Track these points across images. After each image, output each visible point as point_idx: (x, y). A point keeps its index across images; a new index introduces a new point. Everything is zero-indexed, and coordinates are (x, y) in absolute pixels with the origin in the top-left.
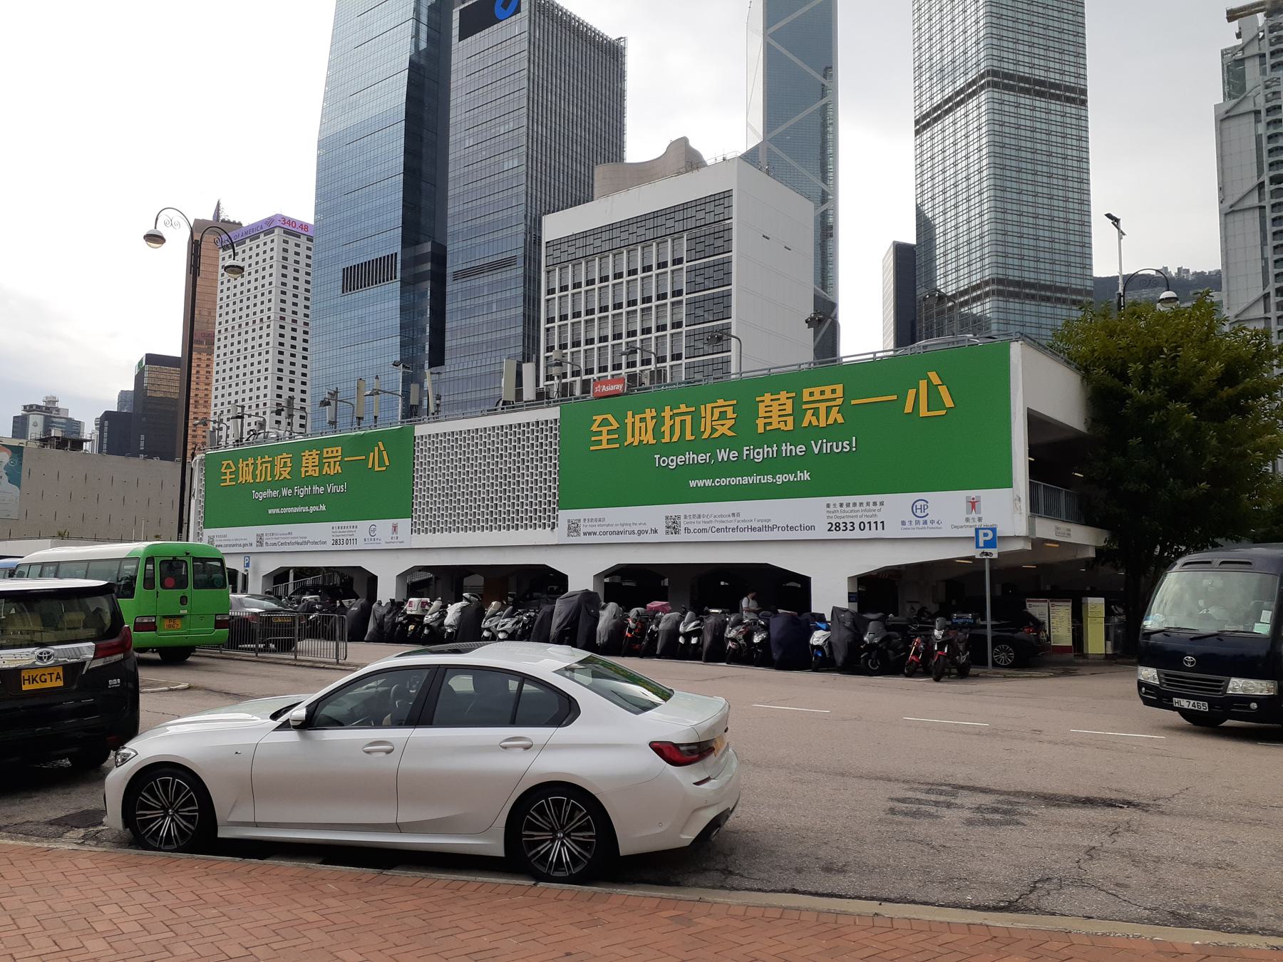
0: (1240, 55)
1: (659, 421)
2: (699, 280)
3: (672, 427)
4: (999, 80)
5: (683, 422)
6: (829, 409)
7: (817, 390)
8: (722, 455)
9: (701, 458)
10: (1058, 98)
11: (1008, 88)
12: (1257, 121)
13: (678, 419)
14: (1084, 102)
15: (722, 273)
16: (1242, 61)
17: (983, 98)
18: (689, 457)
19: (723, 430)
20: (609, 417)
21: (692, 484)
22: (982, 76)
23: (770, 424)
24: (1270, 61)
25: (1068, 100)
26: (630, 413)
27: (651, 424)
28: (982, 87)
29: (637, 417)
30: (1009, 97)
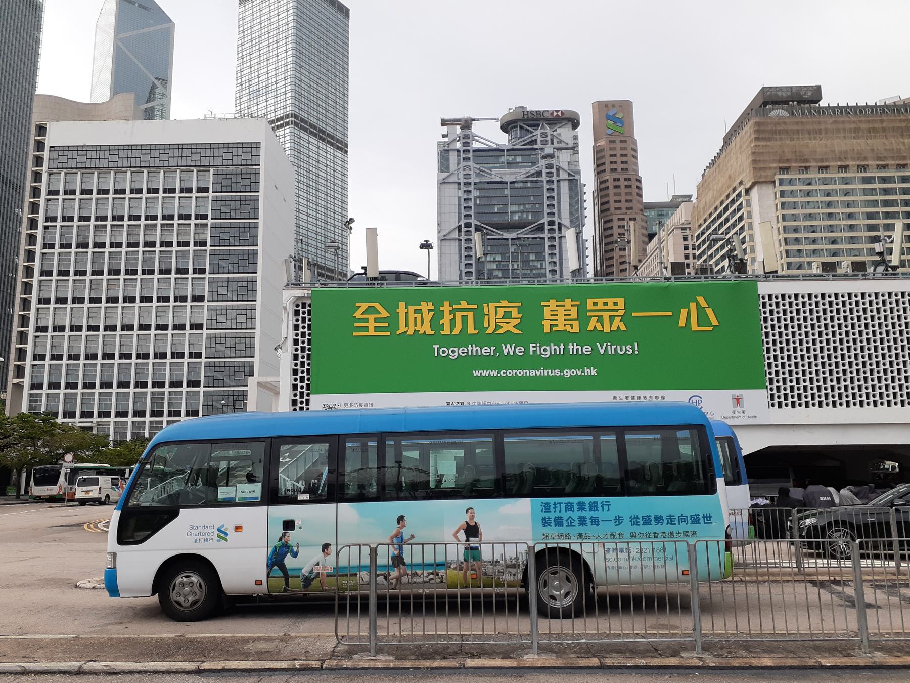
0: (446, 147)
1: (437, 315)
2: (224, 209)
3: (452, 321)
4: (298, 122)
5: (464, 318)
6: (612, 318)
7: (600, 302)
8: (508, 349)
9: (485, 351)
10: (332, 144)
11: (303, 128)
12: (459, 189)
13: (458, 315)
14: (346, 152)
15: (251, 208)
16: (448, 151)
17: (288, 131)
18: (473, 349)
19: (509, 326)
20: (377, 306)
21: (476, 374)
22: (288, 116)
23: (557, 325)
24: (463, 155)
25: (338, 147)
26: (402, 305)
27: (428, 317)
28: (287, 124)
29: (412, 309)
30: (304, 135)
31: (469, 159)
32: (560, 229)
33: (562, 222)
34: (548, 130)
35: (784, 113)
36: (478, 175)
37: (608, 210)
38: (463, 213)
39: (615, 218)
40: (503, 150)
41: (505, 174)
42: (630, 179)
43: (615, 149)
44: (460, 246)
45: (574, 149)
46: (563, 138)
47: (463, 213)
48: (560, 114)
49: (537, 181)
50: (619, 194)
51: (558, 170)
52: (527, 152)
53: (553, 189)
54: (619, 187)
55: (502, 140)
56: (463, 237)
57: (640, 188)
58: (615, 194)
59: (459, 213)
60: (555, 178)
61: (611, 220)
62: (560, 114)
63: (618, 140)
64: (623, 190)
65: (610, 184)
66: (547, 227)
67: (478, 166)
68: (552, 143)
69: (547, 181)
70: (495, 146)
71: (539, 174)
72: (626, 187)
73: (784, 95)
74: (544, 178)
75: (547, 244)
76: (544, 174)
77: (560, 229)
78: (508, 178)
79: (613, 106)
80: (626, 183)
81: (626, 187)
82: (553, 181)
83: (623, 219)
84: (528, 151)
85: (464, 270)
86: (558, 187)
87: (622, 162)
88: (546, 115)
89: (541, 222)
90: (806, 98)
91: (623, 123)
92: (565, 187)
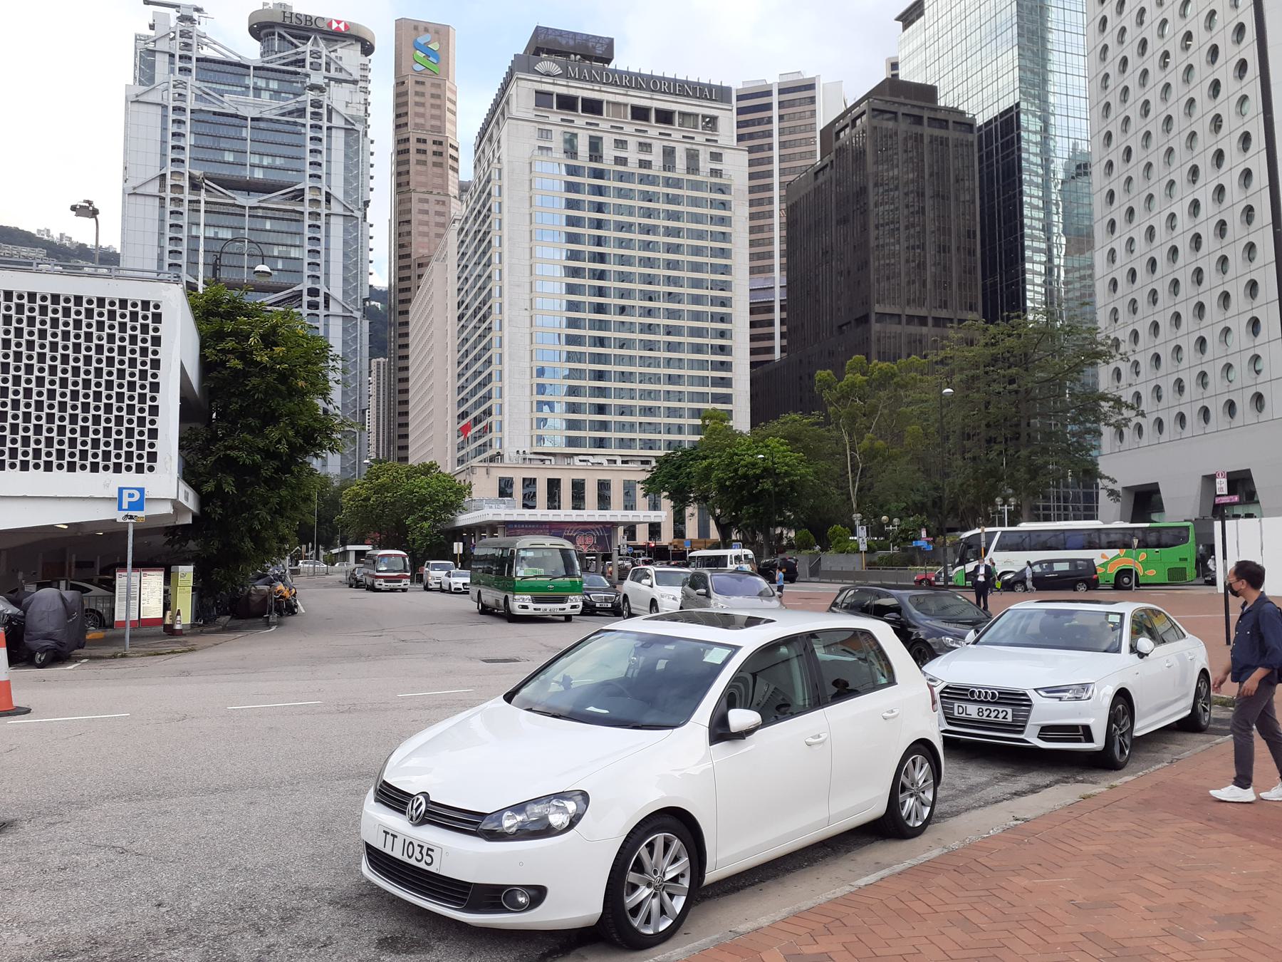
0: (151, 46)
31: (190, 71)
32: (328, 201)
34: (322, 47)
35: (557, 70)
36: (198, 98)
38: (171, 155)
39: (414, 196)
40: (248, 67)
41: (246, 104)
42: (441, 143)
43: (423, 95)
44: (162, 206)
45: (359, 82)
46: (343, 64)
47: (171, 155)
48: (342, 27)
49: (295, 124)
50: (424, 163)
51: (330, 112)
52: (288, 77)
53: (320, 140)
54: (425, 152)
55: (251, 51)
56: (169, 194)
57: (456, 160)
58: (418, 162)
59: (163, 155)
60: (325, 124)
62: (342, 27)
63: (428, 82)
64: (430, 158)
65: (413, 145)
66: (308, 196)
67: (198, 84)
68: (328, 70)
69: (312, 126)
70: (236, 59)
71: (301, 112)
72: (435, 153)
73: (564, 42)
74: (308, 121)
75: (307, 222)
76: (308, 115)
77: (328, 201)
78: (251, 113)
79: (426, 30)
80: (435, 148)
81: (435, 153)
82: (321, 128)
84: (288, 74)
85: (168, 247)
86: (329, 136)
87: (433, 117)
88: (320, 24)
89: (297, 187)
90: (591, 54)
91: (437, 57)
92: (339, 138)
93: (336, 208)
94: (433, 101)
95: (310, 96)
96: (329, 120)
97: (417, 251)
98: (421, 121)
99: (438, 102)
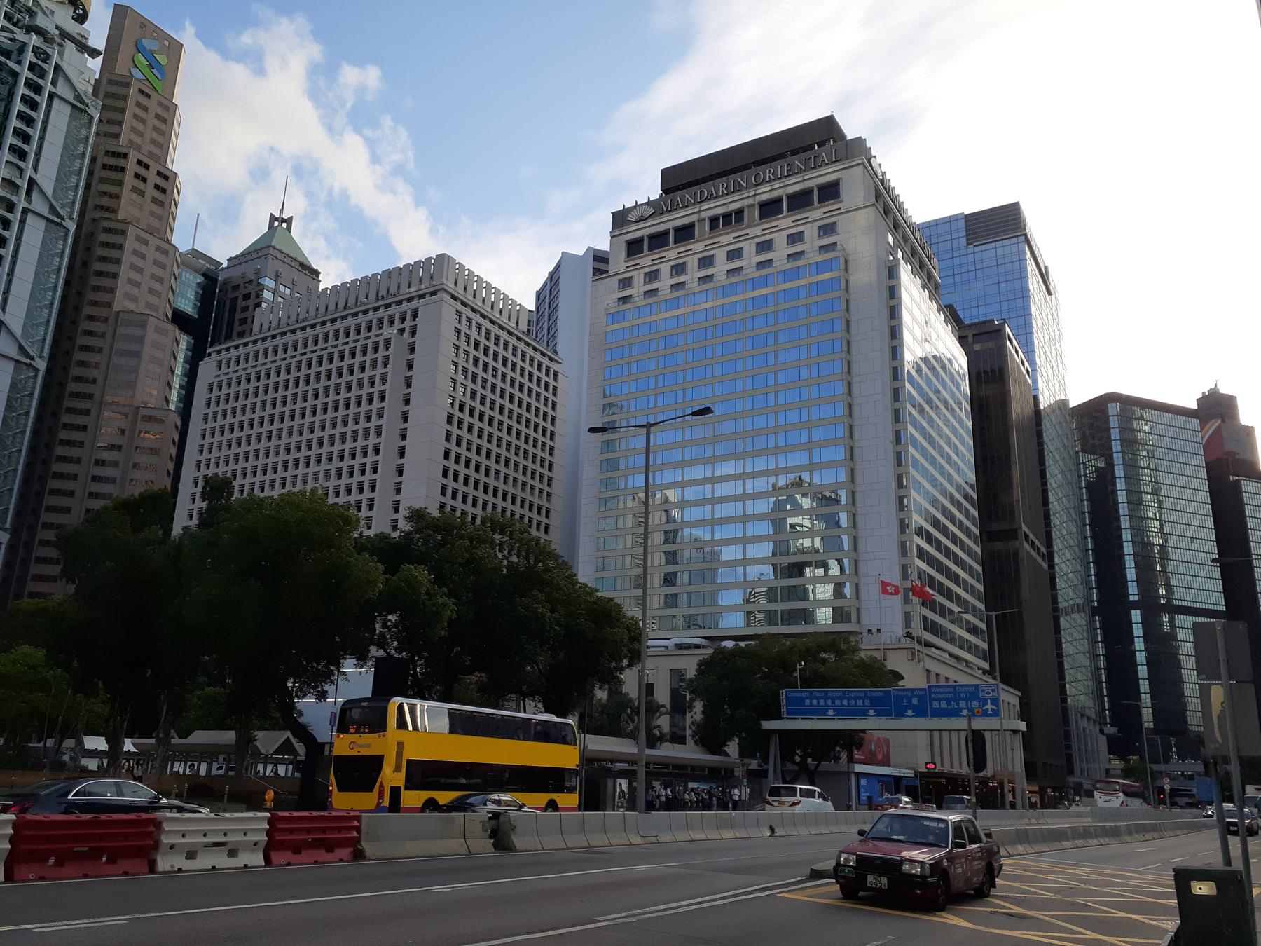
32: (29, 192)
33: (38, 178)
37: (113, 211)
39: (132, 231)
43: (146, 109)
50: (142, 194)
54: (144, 180)
58: (134, 190)
61: (123, 233)
64: (150, 192)
65: (131, 166)
72: (157, 187)
80: (159, 181)
81: (157, 187)
83: (146, 243)
91: (163, 74)
93: (38, 205)
94: (156, 122)
95: (34, 40)
96: (54, 83)
97: (120, 303)
98: (137, 140)
99: (162, 127)
